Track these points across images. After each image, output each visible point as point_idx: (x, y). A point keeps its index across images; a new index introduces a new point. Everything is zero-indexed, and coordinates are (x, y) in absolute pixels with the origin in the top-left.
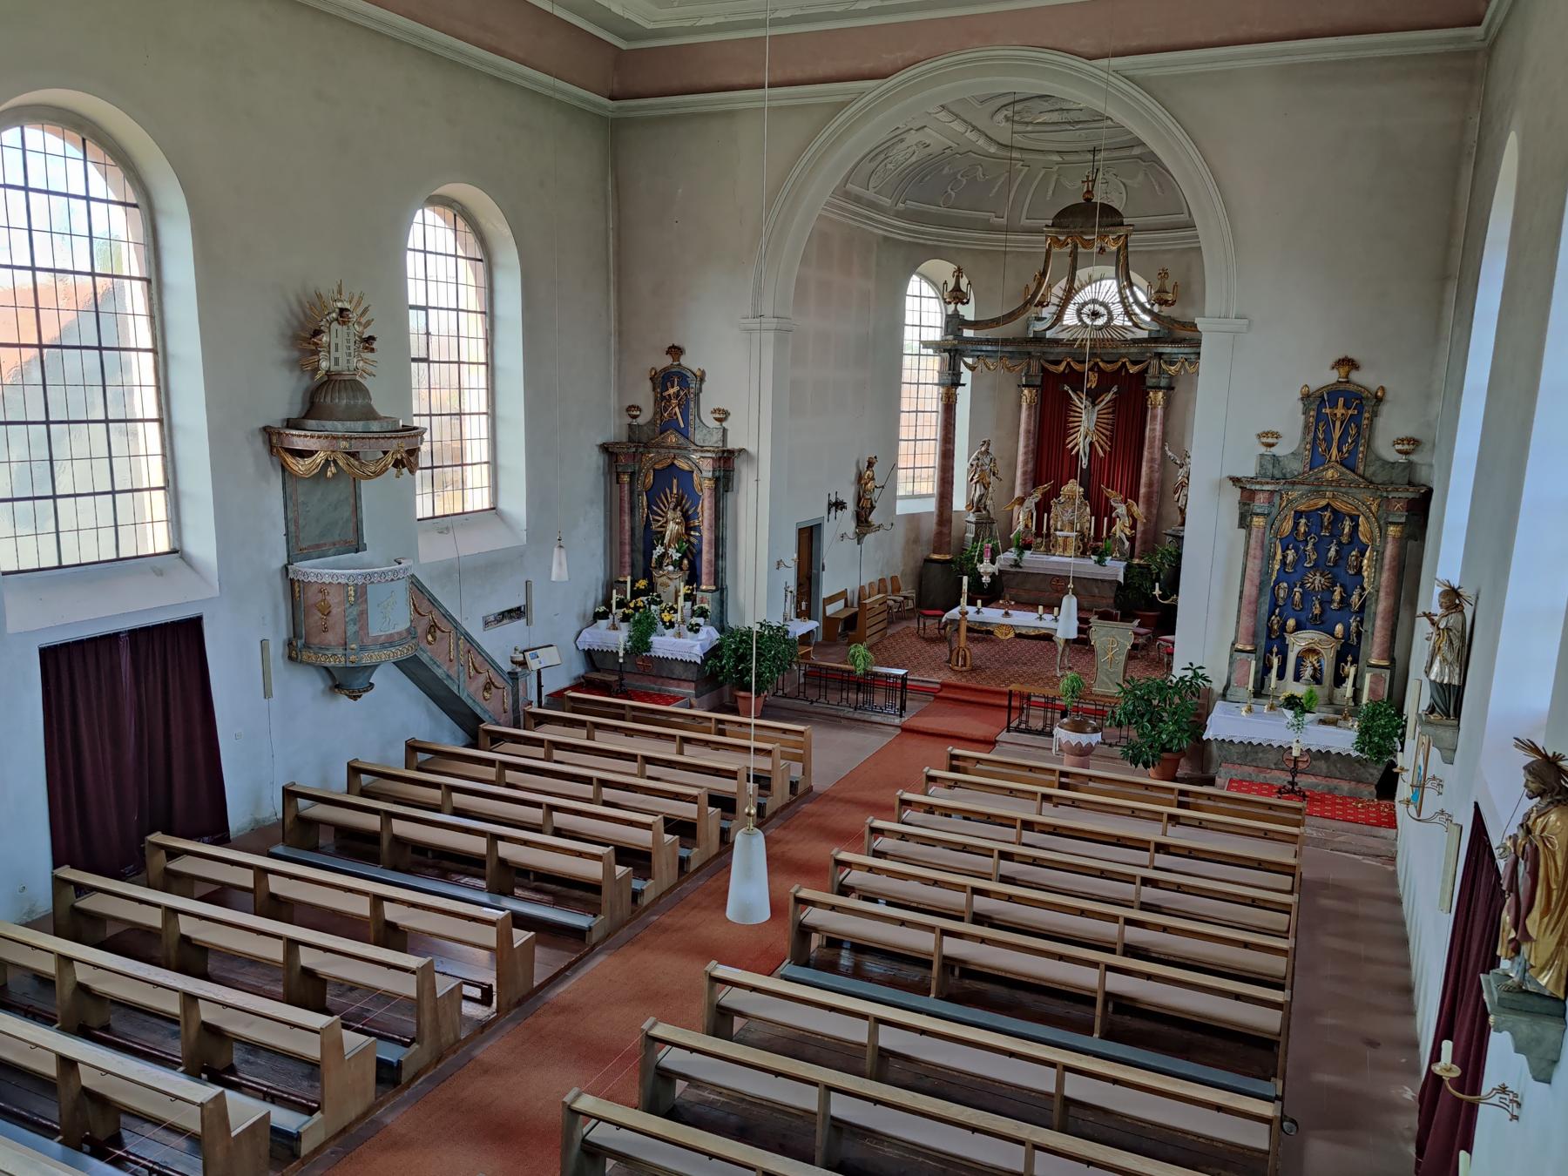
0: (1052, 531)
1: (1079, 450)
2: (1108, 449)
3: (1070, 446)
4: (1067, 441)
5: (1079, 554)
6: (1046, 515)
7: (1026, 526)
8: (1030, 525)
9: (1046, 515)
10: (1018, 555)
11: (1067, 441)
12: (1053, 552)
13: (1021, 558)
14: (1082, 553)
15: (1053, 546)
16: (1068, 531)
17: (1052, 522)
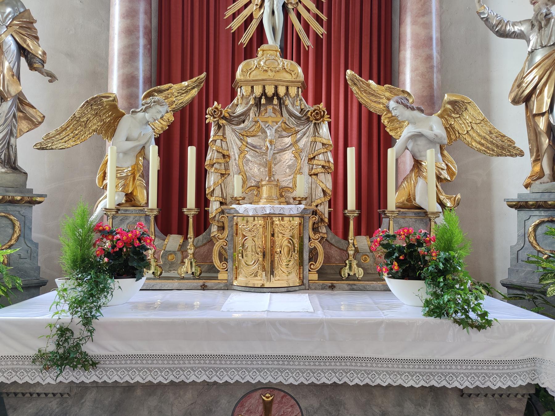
0: (214, 207)
1: (261, 26)
2: (321, 31)
3: (235, 25)
4: (229, 13)
5: (315, 276)
6: (192, 151)
7: (130, 198)
8: (140, 196)
9: (192, 151)
10: (77, 304)
11: (229, 13)
12: (222, 276)
13: (87, 321)
14: (321, 273)
15: (222, 258)
16: (270, 200)
17: (211, 180)
